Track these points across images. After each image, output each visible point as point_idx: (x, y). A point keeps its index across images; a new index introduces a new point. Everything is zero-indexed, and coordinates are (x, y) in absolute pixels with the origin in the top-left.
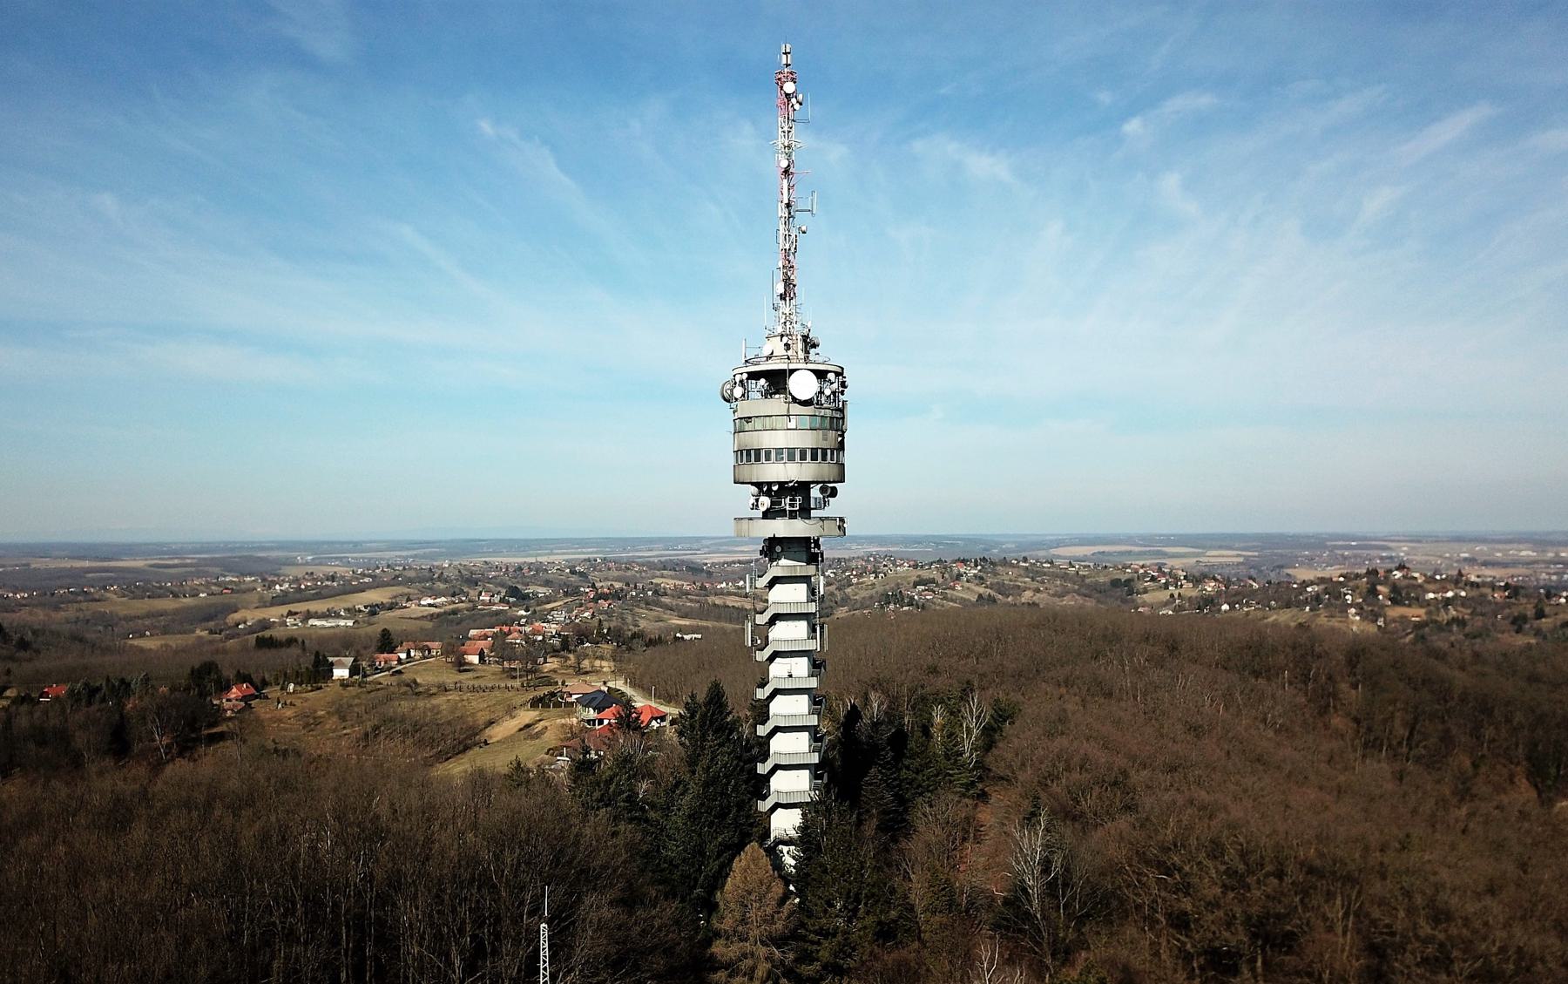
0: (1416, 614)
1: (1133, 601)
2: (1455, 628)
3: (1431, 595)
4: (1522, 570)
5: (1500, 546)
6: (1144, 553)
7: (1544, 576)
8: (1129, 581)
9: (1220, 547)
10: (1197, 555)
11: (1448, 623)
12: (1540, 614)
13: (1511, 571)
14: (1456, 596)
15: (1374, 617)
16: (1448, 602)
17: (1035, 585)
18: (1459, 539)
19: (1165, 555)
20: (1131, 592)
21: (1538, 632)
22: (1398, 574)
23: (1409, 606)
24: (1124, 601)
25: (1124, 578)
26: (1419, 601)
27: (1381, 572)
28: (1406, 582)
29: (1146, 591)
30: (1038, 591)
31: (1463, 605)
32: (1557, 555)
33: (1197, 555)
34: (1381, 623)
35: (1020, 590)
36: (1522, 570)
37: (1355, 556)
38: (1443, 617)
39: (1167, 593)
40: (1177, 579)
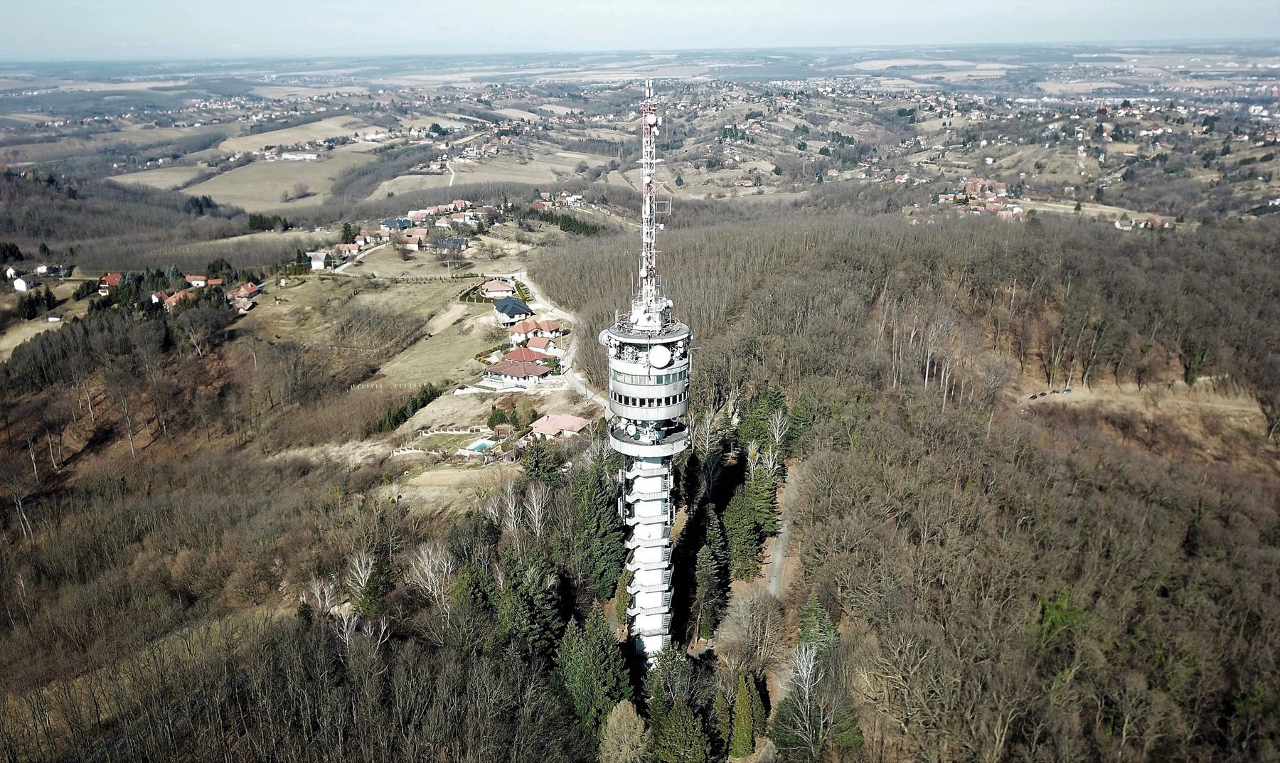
0: (1130, 149)
1: (914, 129)
2: (1158, 163)
3: (1144, 133)
4: (1224, 83)
5: (1211, 57)
6: (928, 67)
7: (1240, 88)
8: (912, 111)
9: (989, 60)
10: (970, 68)
11: (1153, 160)
12: (1226, 151)
13: (1215, 83)
14: (1163, 134)
15: (1098, 152)
16: (1157, 139)
17: (839, 115)
18: (1181, 50)
19: (942, 68)
20: (912, 120)
21: (1221, 168)
22: (1122, 112)
23: (1126, 142)
24: (907, 129)
25: (908, 107)
26: (1134, 138)
27: (1109, 110)
28: (1128, 120)
29: (924, 120)
30: (841, 120)
31: (1168, 141)
32: (1255, 66)
33: (970, 68)
34: (1102, 158)
35: (826, 120)
36: (1224, 83)
37: (1095, 69)
38: (1152, 153)
39: (942, 121)
40: (949, 108)
